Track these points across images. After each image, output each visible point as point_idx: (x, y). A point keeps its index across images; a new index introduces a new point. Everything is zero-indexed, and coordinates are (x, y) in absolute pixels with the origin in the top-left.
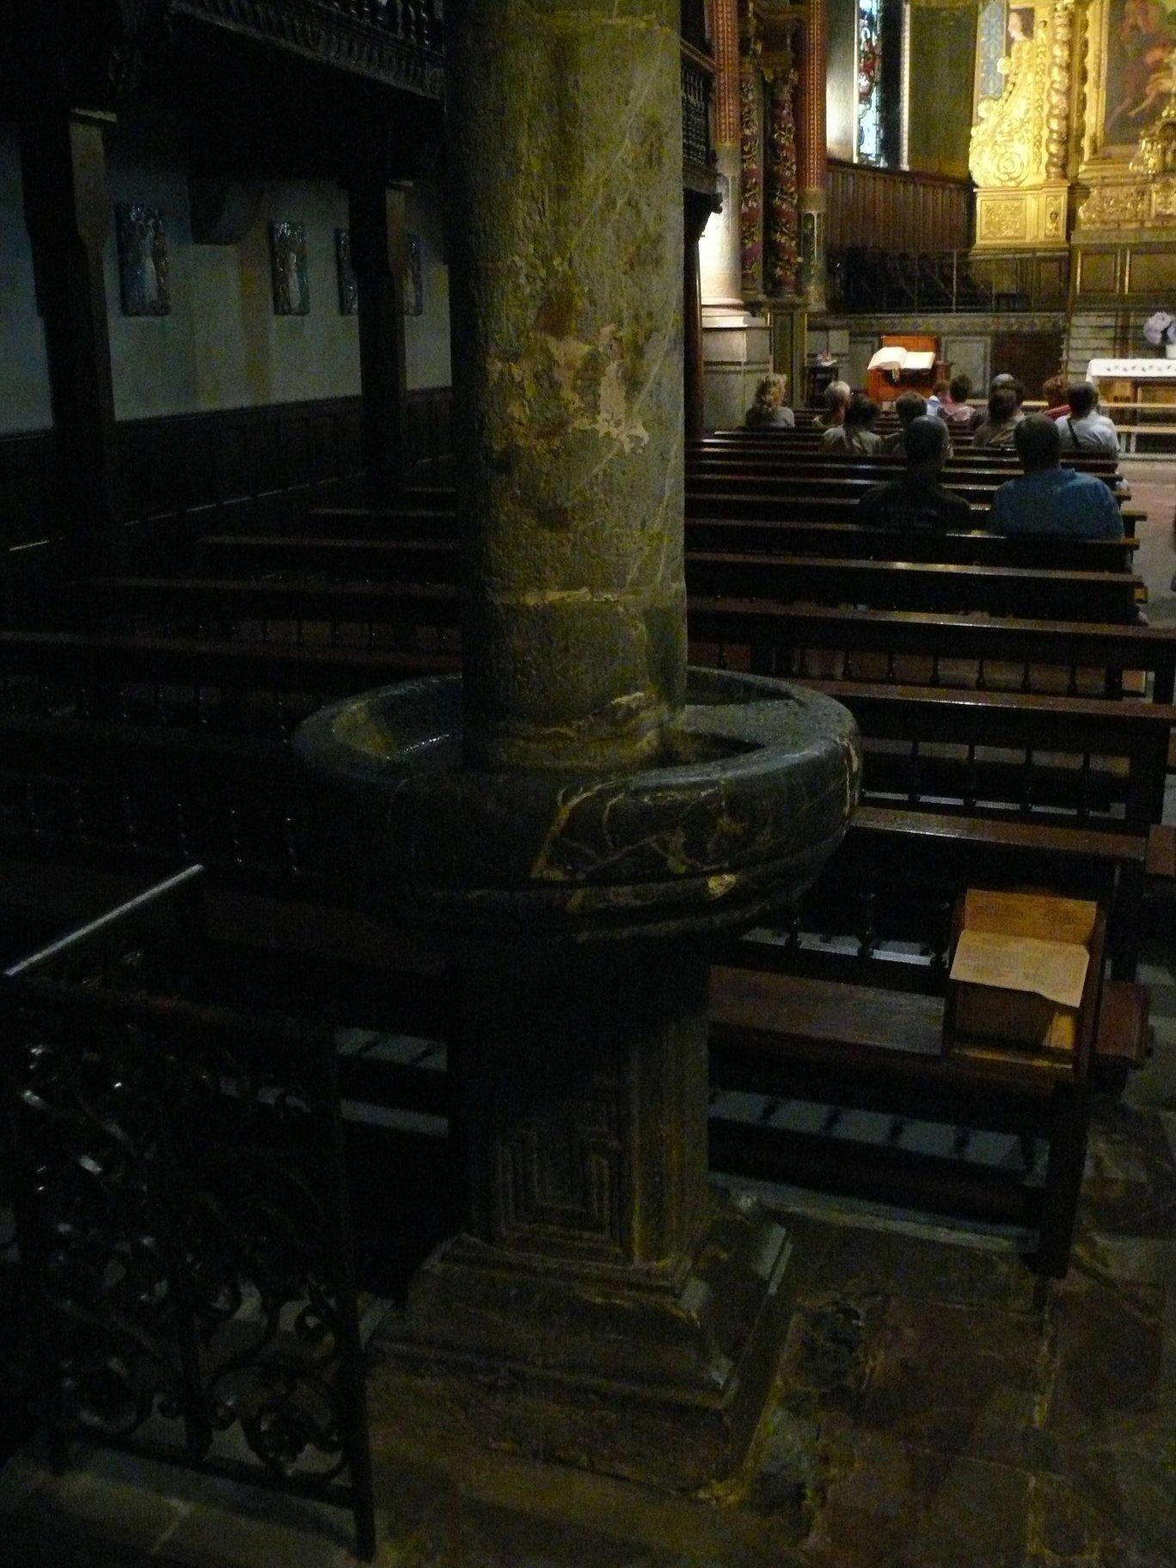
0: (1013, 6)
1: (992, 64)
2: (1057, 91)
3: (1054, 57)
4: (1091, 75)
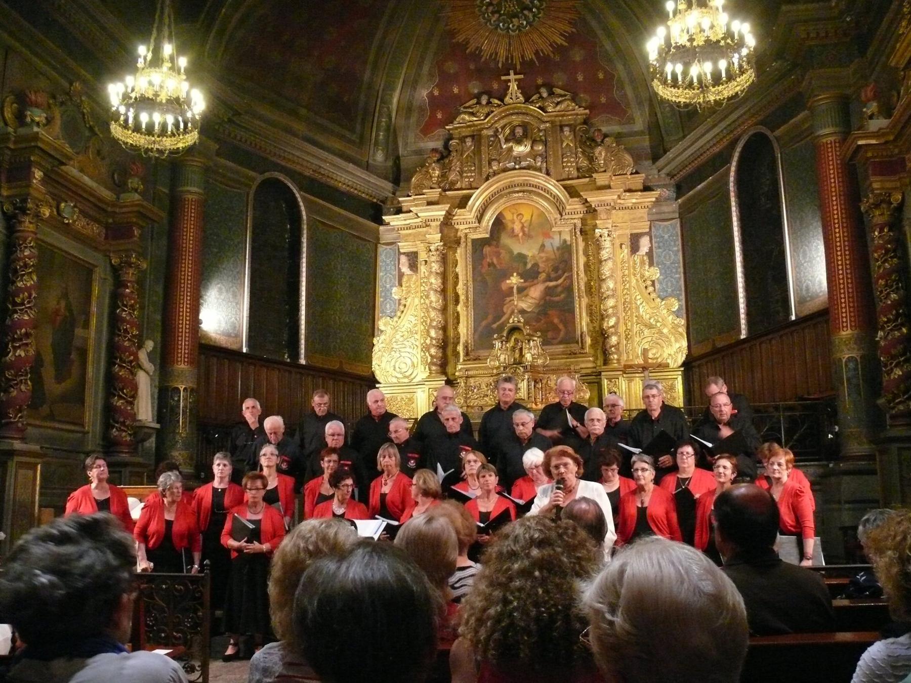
0: (402, 251)
1: (389, 291)
2: (434, 308)
3: (431, 284)
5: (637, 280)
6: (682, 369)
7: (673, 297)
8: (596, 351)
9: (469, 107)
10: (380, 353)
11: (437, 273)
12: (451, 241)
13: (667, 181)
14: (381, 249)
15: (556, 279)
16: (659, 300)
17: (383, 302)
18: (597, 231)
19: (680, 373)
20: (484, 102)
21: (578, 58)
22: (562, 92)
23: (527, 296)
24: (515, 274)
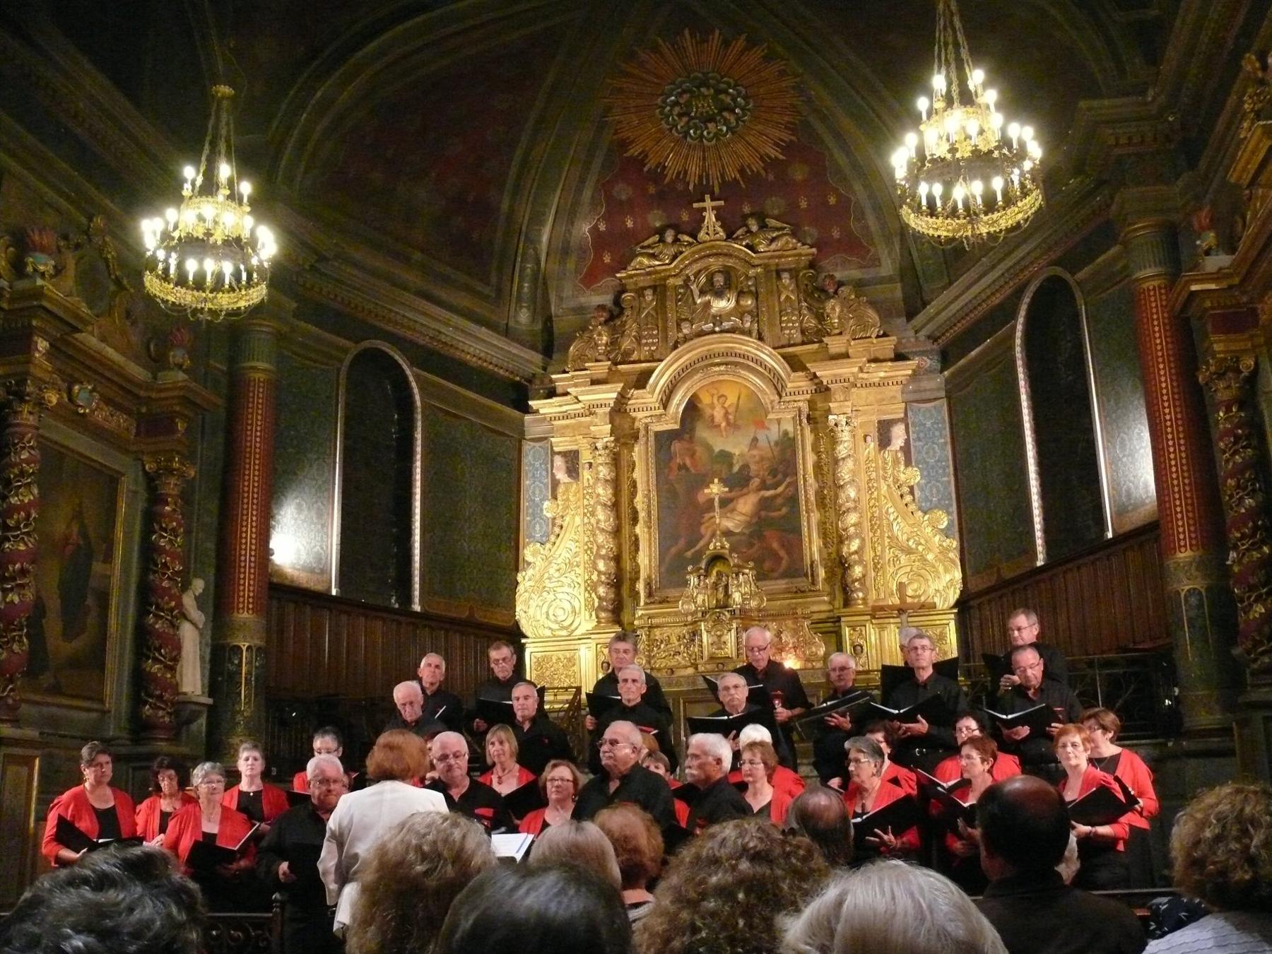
0: (556, 449)
1: (539, 506)
2: (603, 530)
3: (599, 495)
4: (642, 515)
5: (888, 486)
6: (956, 611)
7: (940, 509)
8: (832, 587)
9: (649, 247)
10: (526, 594)
11: (607, 481)
12: (625, 434)
13: (929, 346)
14: (527, 447)
15: (775, 486)
16: (920, 513)
17: (530, 521)
18: (831, 417)
19: (953, 616)
20: (669, 239)
21: (799, 177)
22: (779, 224)
23: (733, 510)
24: (716, 480)
